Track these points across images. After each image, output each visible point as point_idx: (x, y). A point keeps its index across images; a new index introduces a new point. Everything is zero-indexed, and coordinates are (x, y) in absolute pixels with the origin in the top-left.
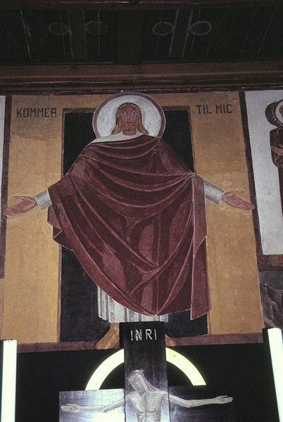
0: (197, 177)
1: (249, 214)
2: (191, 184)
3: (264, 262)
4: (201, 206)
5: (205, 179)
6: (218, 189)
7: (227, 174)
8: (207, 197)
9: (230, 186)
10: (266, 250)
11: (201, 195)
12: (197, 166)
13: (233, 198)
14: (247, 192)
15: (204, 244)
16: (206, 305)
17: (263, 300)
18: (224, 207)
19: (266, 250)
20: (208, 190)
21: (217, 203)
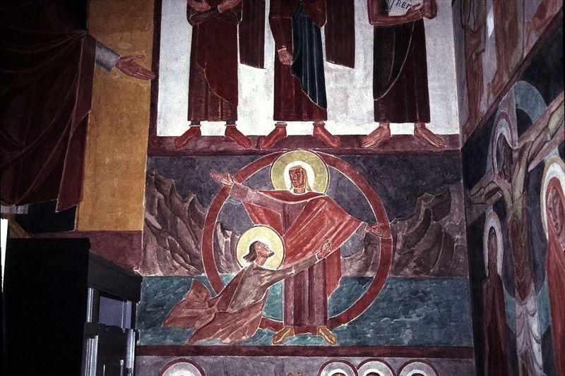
0: (89, 37)
1: (146, 86)
2: (78, 48)
3: (157, 145)
4: (89, 73)
5: (99, 39)
6: (112, 51)
7: (126, 34)
8: (98, 61)
9: (129, 50)
10: (162, 131)
11: (90, 60)
12: (91, 23)
13: (130, 64)
14: (149, 57)
15: (85, 122)
16: (78, 195)
17: (147, 193)
18: (117, 75)
19: (162, 131)
20: (101, 54)
21: (109, 69)
